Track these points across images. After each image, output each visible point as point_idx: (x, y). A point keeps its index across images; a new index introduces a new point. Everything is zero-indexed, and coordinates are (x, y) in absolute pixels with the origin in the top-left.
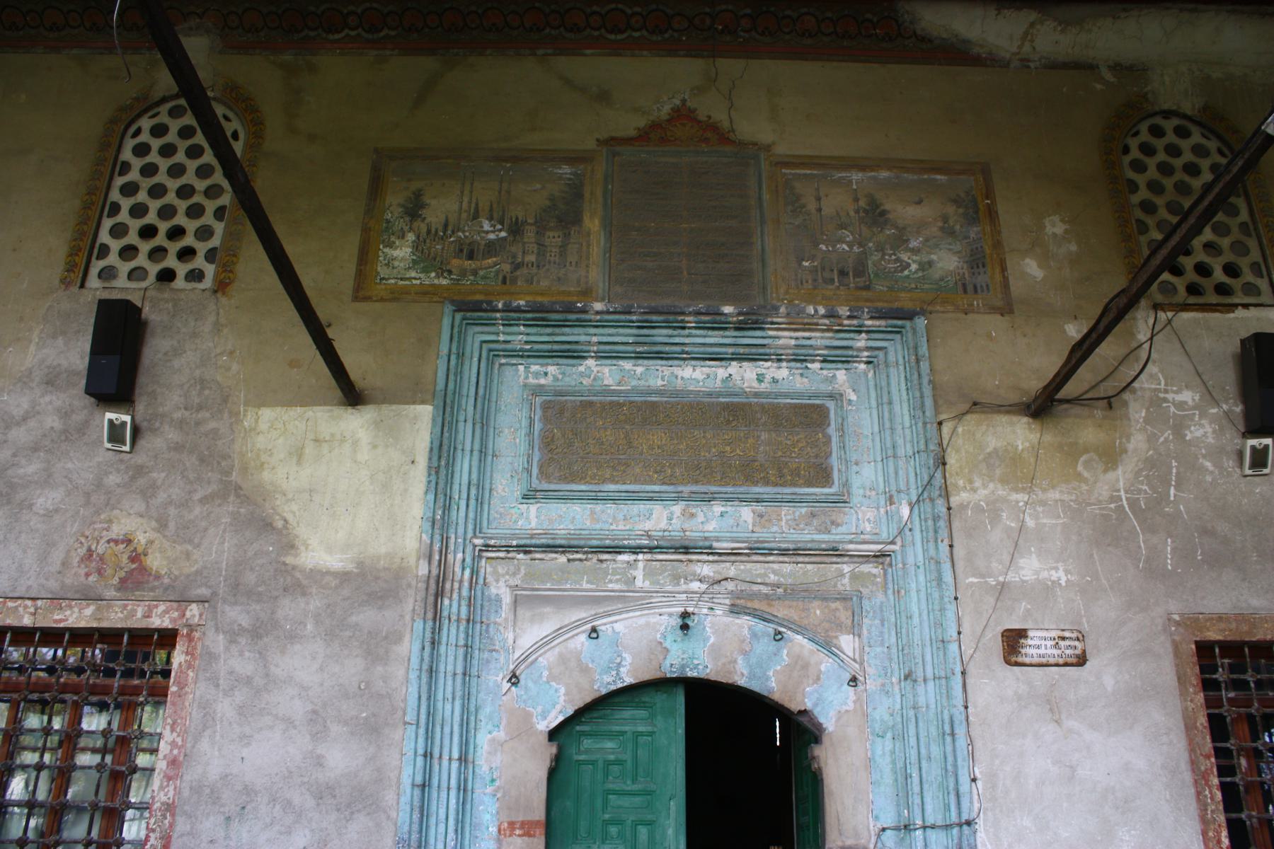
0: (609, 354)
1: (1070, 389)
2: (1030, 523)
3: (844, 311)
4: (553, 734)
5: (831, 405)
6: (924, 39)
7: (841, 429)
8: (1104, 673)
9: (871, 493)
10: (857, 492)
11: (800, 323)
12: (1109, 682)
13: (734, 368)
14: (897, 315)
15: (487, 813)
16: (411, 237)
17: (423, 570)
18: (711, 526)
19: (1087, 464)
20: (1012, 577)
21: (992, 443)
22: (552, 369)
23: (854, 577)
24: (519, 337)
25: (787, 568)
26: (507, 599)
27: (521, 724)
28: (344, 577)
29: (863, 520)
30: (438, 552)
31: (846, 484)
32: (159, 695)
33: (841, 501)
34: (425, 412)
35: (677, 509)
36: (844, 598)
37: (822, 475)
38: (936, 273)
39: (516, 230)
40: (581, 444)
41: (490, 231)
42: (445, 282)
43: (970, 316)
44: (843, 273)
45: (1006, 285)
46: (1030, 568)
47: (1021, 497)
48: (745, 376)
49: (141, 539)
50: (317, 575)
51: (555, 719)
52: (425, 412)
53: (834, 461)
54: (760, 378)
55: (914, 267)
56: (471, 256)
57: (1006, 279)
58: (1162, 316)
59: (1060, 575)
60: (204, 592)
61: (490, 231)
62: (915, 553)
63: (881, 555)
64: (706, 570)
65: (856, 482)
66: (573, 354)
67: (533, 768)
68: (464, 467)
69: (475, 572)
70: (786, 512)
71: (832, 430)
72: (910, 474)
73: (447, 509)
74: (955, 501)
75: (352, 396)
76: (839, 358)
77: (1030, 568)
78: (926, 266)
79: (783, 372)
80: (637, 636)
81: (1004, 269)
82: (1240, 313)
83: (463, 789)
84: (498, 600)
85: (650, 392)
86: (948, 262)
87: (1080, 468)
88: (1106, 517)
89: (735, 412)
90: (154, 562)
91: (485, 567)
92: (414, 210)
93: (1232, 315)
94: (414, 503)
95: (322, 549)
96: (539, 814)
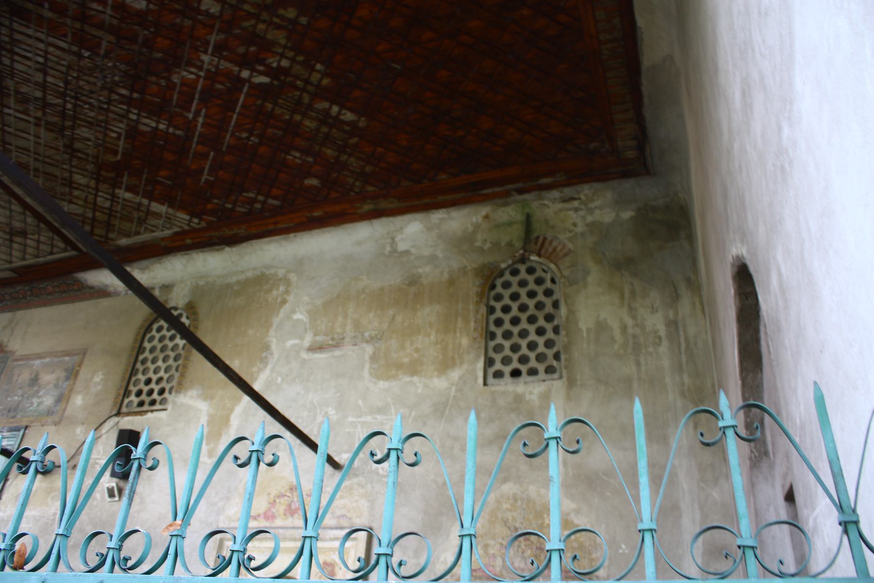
6: (91, 288)
19: (53, 499)
38: (41, 407)
43: (45, 427)
45: (64, 410)
55: (35, 405)
57: (66, 406)
58: (116, 419)
81: (68, 402)
82: (149, 415)
87: (49, 500)
88: (47, 523)
93: (145, 417)
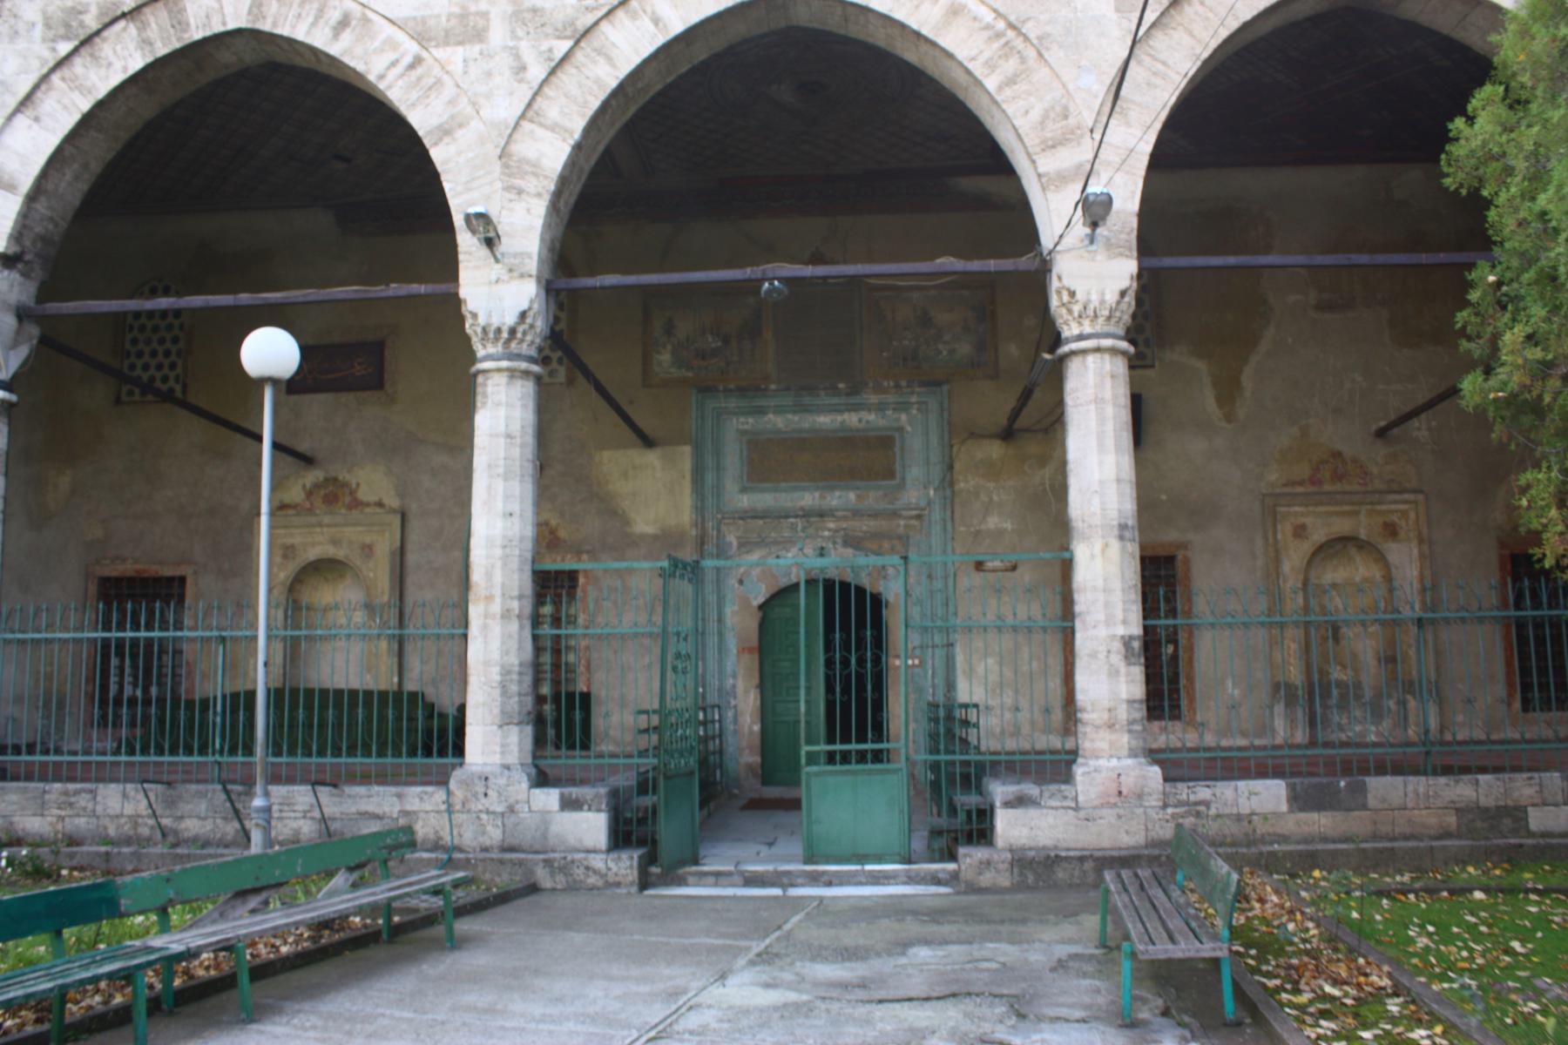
0: (779, 410)
1: (1022, 422)
2: (995, 498)
3: (904, 383)
4: (761, 607)
5: (897, 436)
7: (902, 448)
8: (1025, 576)
9: (917, 486)
10: (909, 482)
11: (879, 389)
12: (1027, 578)
13: (846, 416)
14: (933, 383)
15: (732, 644)
16: (669, 347)
17: (694, 532)
18: (834, 503)
20: (983, 527)
21: (979, 455)
22: (751, 420)
23: (906, 526)
24: (732, 403)
25: (872, 523)
26: (735, 543)
27: (745, 602)
28: (655, 537)
29: (912, 496)
30: (700, 522)
31: (903, 479)
32: (572, 596)
33: (902, 486)
34: (687, 450)
35: (817, 494)
36: (900, 538)
37: (890, 474)
39: (726, 341)
40: (770, 461)
41: (713, 342)
42: (690, 374)
44: (905, 359)
46: (993, 522)
47: (991, 485)
48: (852, 419)
49: (553, 523)
50: (643, 537)
51: (761, 600)
52: (687, 450)
53: (898, 466)
54: (860, 421)
56: (703, 358)
59: (1008, 526)
60: (587, 547)
61: (713, 342)
62: (937, 515)
63: (919, 517)
64: (832, 525)
65: (909, 477)
66: (761, 411)
67: (753, 624)
68: (710, 478)
69: (719, 531)
70: (872, 494)
71: (897, 450)
72: (936, 472)
73: (702, 501)
74: (957, 488)
75: (648, 442)
76: (903, 407)
77: (993, 522)
78: (952, 352)
79: (872, 417)
80: (797, 561)
81: (996, 350)
83: (721, 634)
84: (730, 544)
85: (801, 431)
86: (965, 349)
89: (847, 441)
90: (562, 534)
91: (723, 528)
92: (669, 330)
94: (687, 500)
95: (644, 524)
96: (755, 642)
